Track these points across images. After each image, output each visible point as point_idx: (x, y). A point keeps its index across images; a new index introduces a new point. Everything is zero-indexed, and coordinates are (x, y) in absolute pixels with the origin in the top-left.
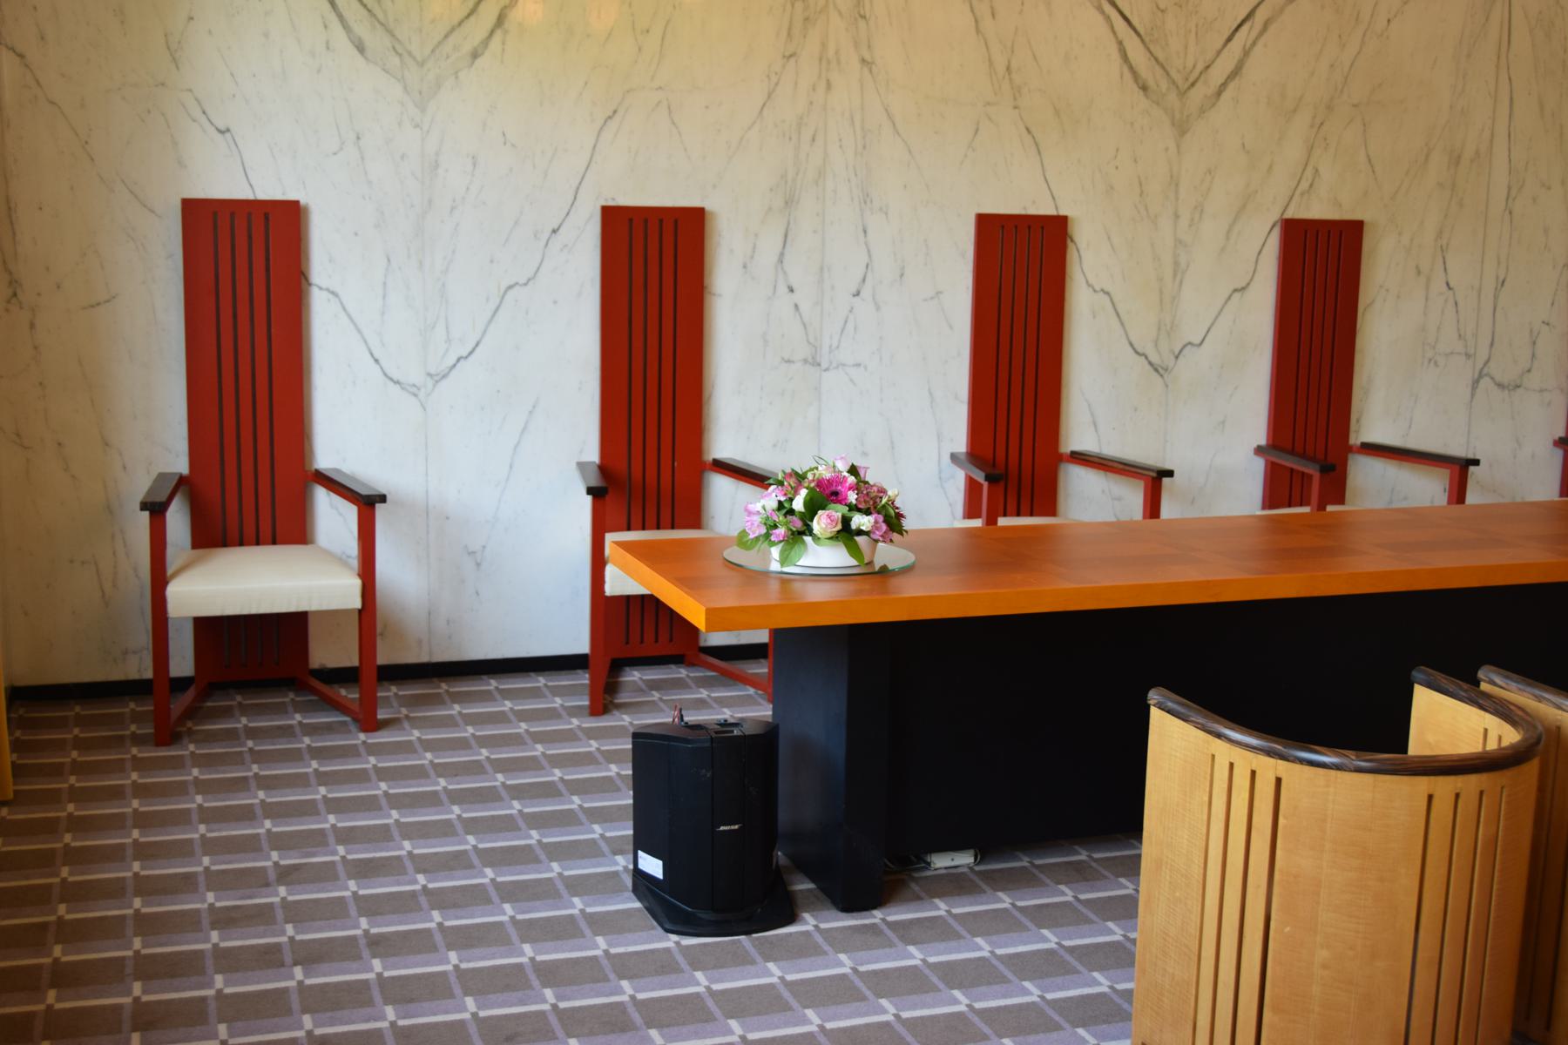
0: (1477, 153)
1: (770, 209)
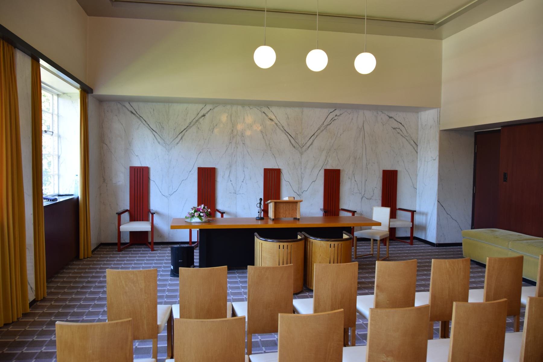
0: (360, 157)
1: (227, 168)
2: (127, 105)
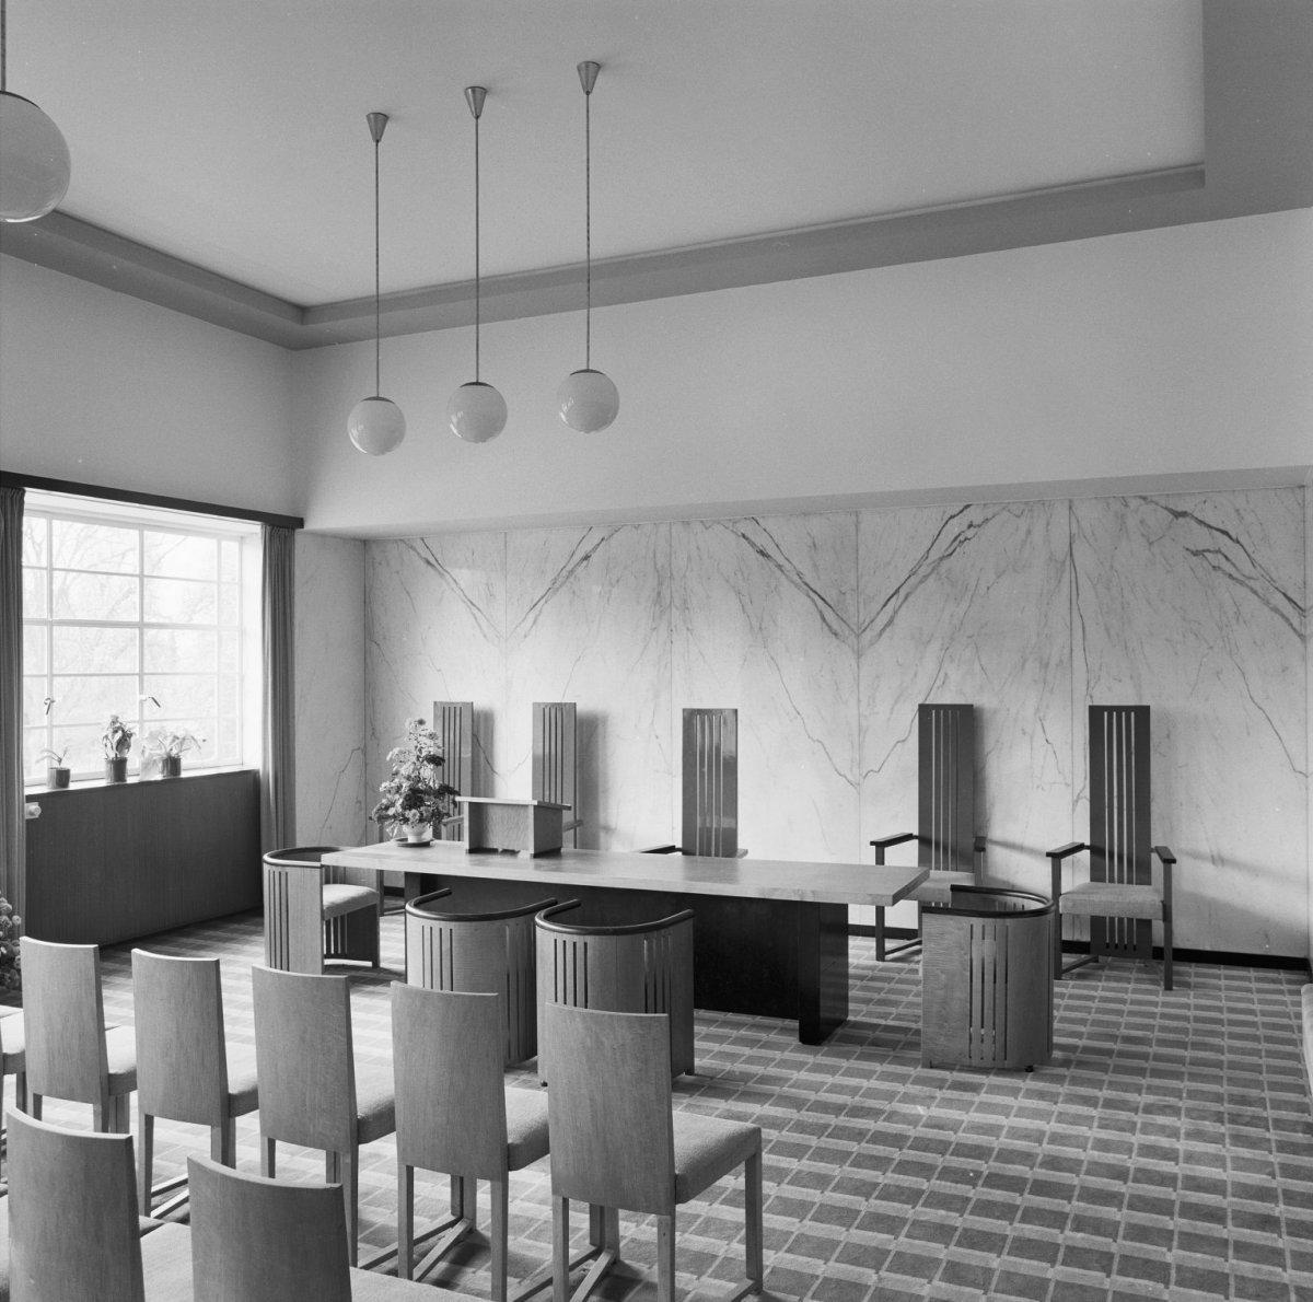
0: (1061, 661)
2: (419, 545)
